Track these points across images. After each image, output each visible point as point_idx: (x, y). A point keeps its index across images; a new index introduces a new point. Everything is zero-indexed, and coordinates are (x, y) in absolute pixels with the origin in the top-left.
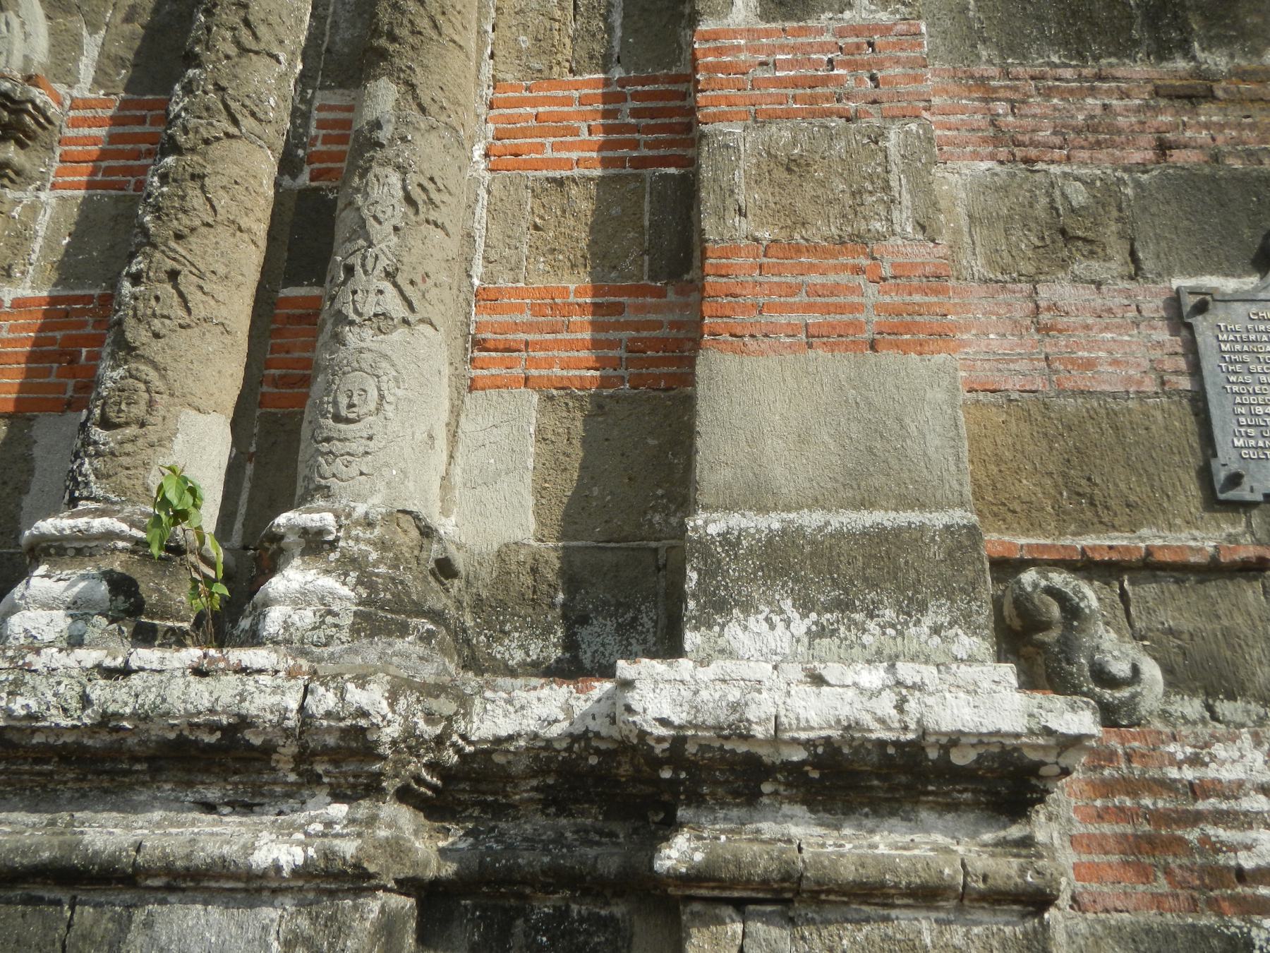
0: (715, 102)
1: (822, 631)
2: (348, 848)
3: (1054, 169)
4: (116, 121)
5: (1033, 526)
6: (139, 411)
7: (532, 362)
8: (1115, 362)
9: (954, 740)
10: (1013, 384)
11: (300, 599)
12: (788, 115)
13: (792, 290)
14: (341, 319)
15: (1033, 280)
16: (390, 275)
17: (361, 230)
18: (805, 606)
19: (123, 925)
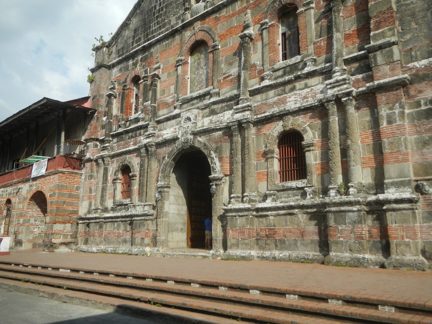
0: (383, 136)
1: (397, 190)
2: (360, 209)
3: (424, 135)
4: (322, 142)
5: (421, 176)
6: (335, 176)
7: (369, 165)
8: (430, 158)
9: (405, 198)
10: (419, 162)
11: (352, 191)
12: (391, 137)
13: (392, 157)
14: (350, 166)
15: (421, 149)
16: (354, 161)
17: (350, 157)
18: (395, 187)
19: (345, 214)
